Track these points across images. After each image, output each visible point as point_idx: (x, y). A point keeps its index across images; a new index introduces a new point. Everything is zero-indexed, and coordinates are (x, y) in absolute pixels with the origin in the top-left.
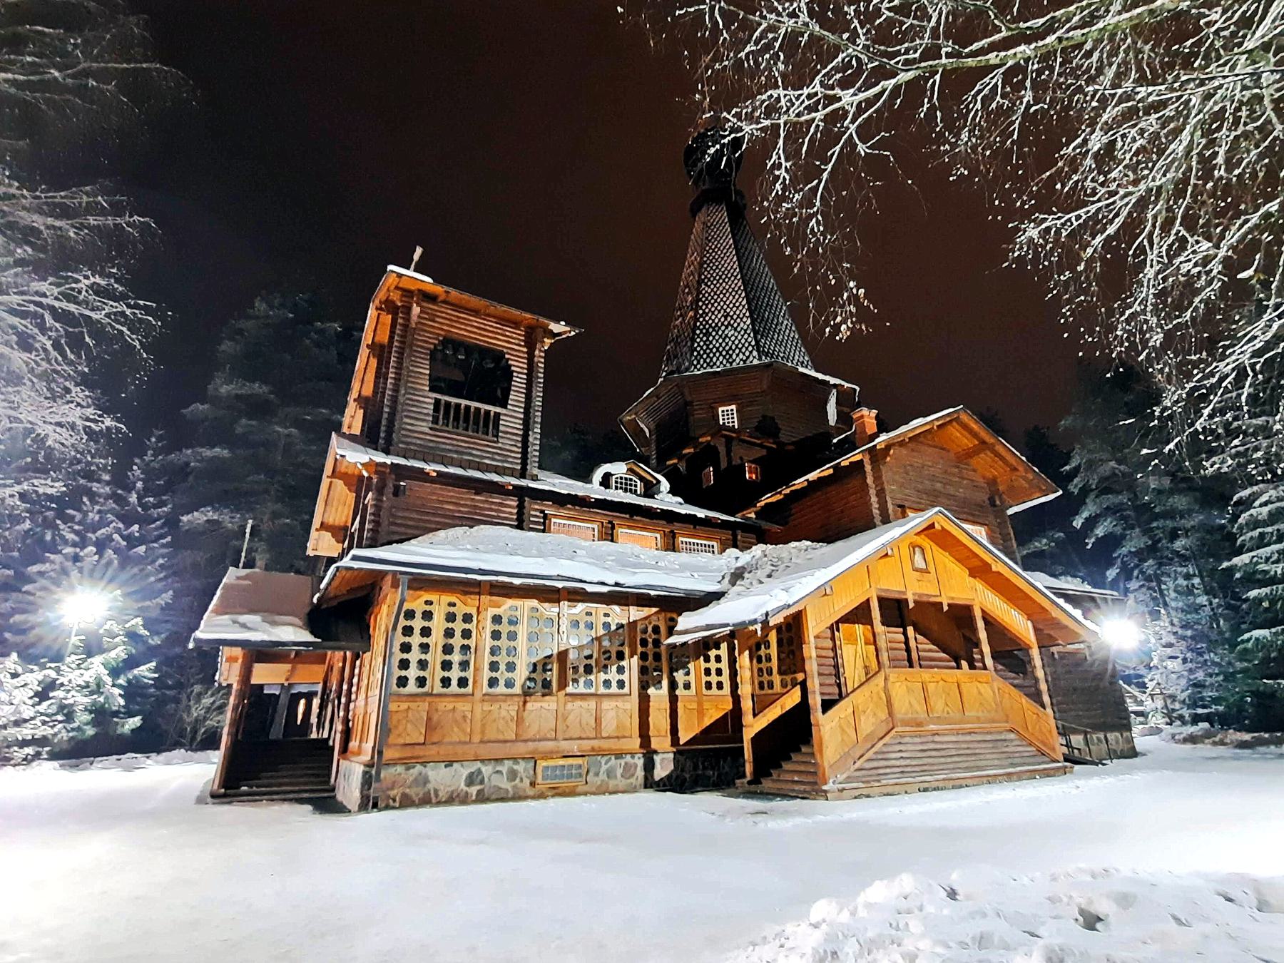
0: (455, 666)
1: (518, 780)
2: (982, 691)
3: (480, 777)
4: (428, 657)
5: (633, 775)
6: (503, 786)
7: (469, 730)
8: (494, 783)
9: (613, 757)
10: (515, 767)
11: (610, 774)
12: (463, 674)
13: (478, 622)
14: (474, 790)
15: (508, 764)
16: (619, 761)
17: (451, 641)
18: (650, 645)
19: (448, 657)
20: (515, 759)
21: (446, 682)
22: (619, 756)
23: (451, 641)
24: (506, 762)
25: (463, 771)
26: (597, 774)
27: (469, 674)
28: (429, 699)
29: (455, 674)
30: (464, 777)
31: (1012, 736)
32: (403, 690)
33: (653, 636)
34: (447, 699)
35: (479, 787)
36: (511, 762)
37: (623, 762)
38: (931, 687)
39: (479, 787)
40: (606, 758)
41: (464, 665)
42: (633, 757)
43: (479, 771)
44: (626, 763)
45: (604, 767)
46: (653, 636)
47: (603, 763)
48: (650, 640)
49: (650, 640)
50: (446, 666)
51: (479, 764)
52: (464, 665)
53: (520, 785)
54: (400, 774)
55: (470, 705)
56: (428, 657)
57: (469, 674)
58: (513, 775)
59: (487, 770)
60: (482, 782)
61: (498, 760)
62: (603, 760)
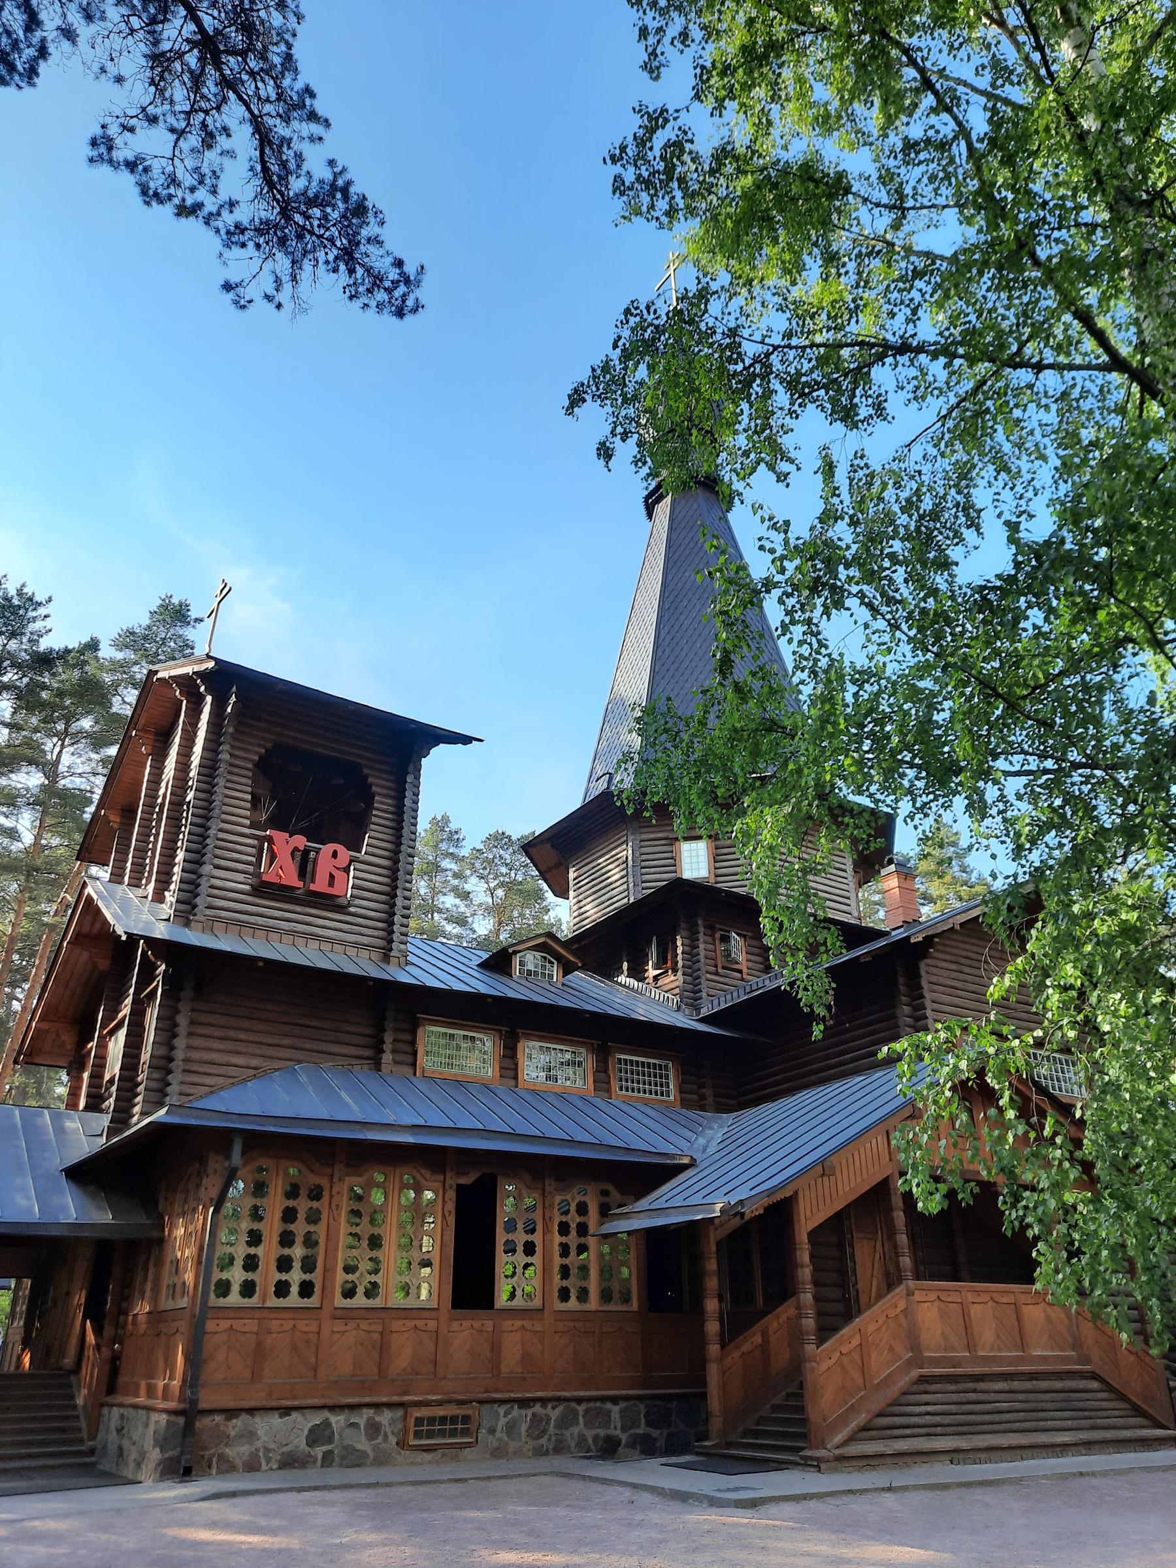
0: (297, 1265)
1: (380, 1439)
2: (1053, 1315)
3: (327, 1432)
4: (259, 1251)
5: (544, 1432)
6: (359, 1447)
7: (313, 1359)
8: (349, 1442)
9: (516, 1407)
10: (377, 1419)
11: (511, 1429)
12: (307, 1277)
13: (331, 1196)
14: (319, 1451)
15: (368, 1413)
16: (524, 1412)
17: (292, 1227)
18: (573, 1233)
19: (287, 1251)
20: (377, 1406)
21: (282, 1289)
22: (524, 1403)
23: (292, 1227)
24: (365, 1411)
25: (305, 1422)
26: (492, 1431)
27: (316, 1277)
28: (258, 1315)
29: (296, 1276)
30: (306, 1432)
31: (1095, 1385)
32: (222, 1302)
33: (578, 1219)
34: (281, 1315)
35: (325, 1448)
36: (371, 1411)
37: (529, 1412)
38: (975, 1310)
39: (325, 1448)
40: (507, 1406)
41: (308, 1265)
42: (544, 1406)
43: (327, 1424)
44: (534, 1415)
45: (503, 1421)
46: (578, 1219)
47: (502, 1413)
48: (573, 1226)
49: (573, 1226)
50: (284, 1264)
51: (326, 1414)
52: (308, 1265)
53: (384, 1446)
54: (218, 1425)
55: (316, 1323)
56: (259, 1251)
57: (316, 1277)
58: (374, 1429)
59: (337, 1421)
60: (330, 1440)
61: (352, 1407)
62: (501, 1410)
